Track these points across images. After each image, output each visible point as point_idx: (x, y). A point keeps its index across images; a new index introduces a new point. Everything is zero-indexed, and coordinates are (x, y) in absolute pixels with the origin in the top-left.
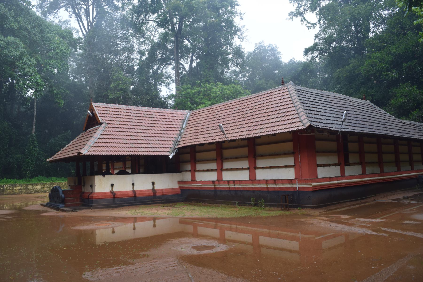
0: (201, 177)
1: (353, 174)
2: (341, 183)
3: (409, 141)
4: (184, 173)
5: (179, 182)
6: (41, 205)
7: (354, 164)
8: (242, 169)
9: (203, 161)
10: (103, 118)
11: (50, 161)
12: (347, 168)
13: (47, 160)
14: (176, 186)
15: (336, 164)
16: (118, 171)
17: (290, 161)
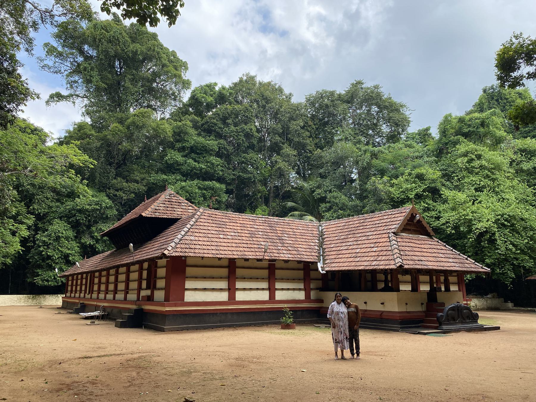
9: (405, 282)
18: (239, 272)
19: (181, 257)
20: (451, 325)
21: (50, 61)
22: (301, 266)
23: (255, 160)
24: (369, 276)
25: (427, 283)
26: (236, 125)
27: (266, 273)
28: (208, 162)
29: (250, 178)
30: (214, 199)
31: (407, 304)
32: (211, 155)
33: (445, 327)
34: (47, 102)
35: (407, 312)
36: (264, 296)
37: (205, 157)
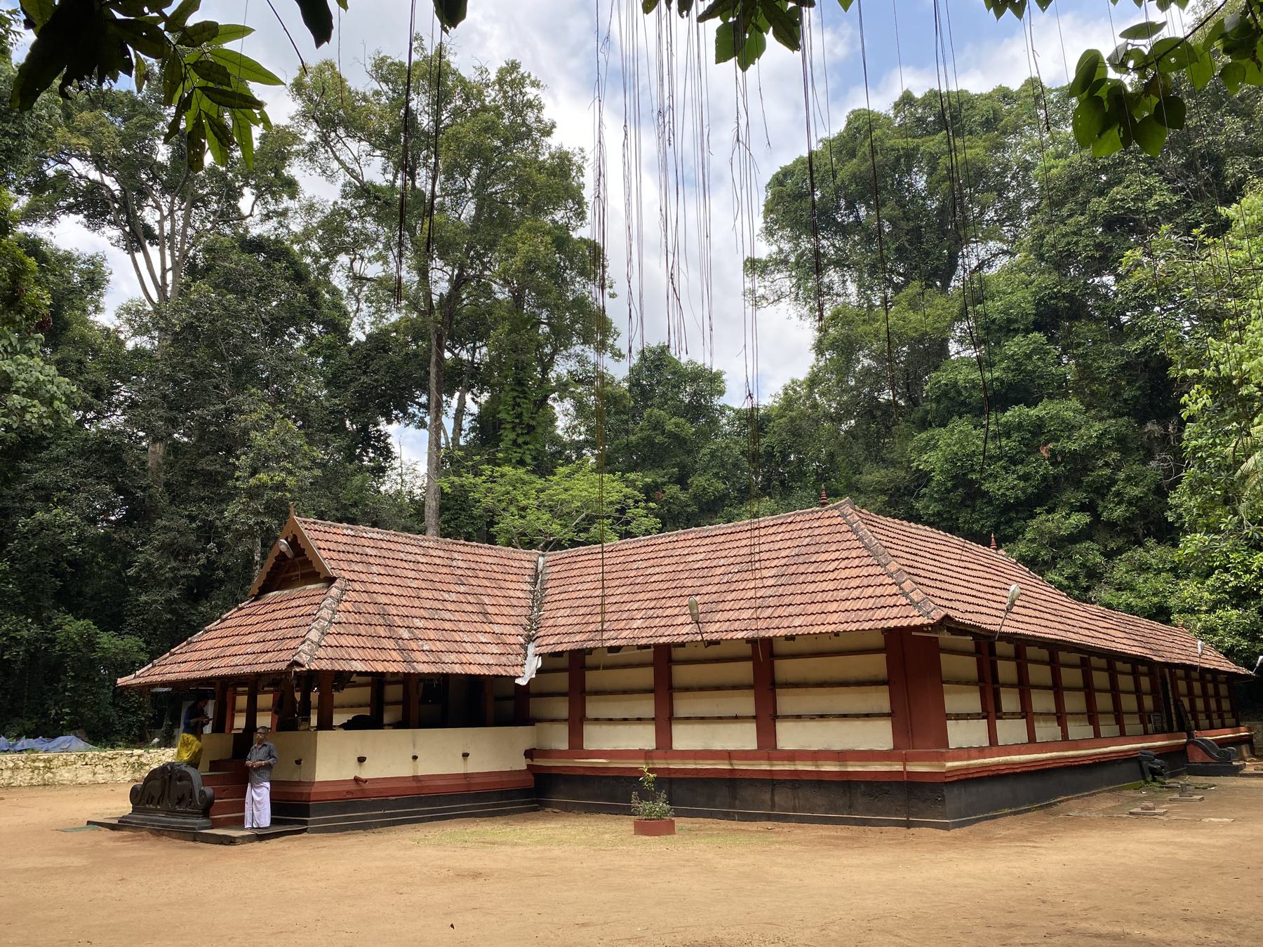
0: (599, 739)
1: (1014, 743)
2: (998, 764)
3: (1112, 657)
4: (546, 726)
5: (529, 754)
6: (89, 823)
7: (1013, 715)
8: (736, 718)
10: (334, 564)
11: (126, 687)
12: (998, 722)
13: (120, 681)
14: (521, 764)
15: (1013, 714)
16: (350, 717)
17: (880, 700)
21: (762, 286)
25: (968, 683)
30: (1044, 452)
32: (1016, 331)
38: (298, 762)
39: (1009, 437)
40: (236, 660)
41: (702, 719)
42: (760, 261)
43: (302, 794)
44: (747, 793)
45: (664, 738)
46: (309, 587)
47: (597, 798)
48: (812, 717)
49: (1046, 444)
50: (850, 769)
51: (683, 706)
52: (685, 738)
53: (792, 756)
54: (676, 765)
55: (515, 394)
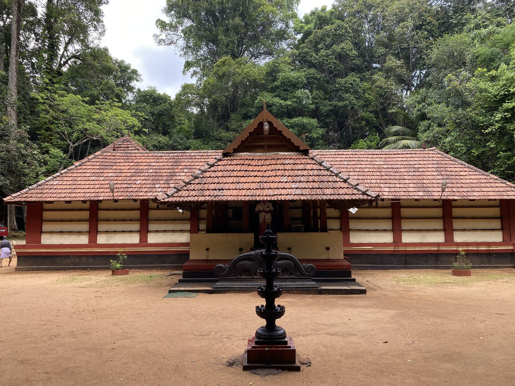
8: (435, 230)
18: (102, 214)
19: (39, 202)
20: (240, 281)
22: (138, 205)
23: (351, 84)
24: (299, 213)
26: (328, 47)
27: (136, 214)
28: (295, 97)
29: (345, 106)
31: (207, 249)
32: (298, 88)
33: (219, 284)
34: (184, 72)
35: (207, 261)
36: (135, 239)
37: (293, 92)
38: (328, 249)
39: (292, 127)
40: (271, 192)
41: (419, 230)
42: (165, 23)
43: (341, 266)
44: (444, 259)
45: (93, 240)
46: (280, 153)
47: (364, 263)
48: (470, 230)
49: (304, 134)
50: (491, 249)
51: (405, 225)
52: (407, 238)
53: (458, 244)
54: (401, 249)
55: (52, 53)
